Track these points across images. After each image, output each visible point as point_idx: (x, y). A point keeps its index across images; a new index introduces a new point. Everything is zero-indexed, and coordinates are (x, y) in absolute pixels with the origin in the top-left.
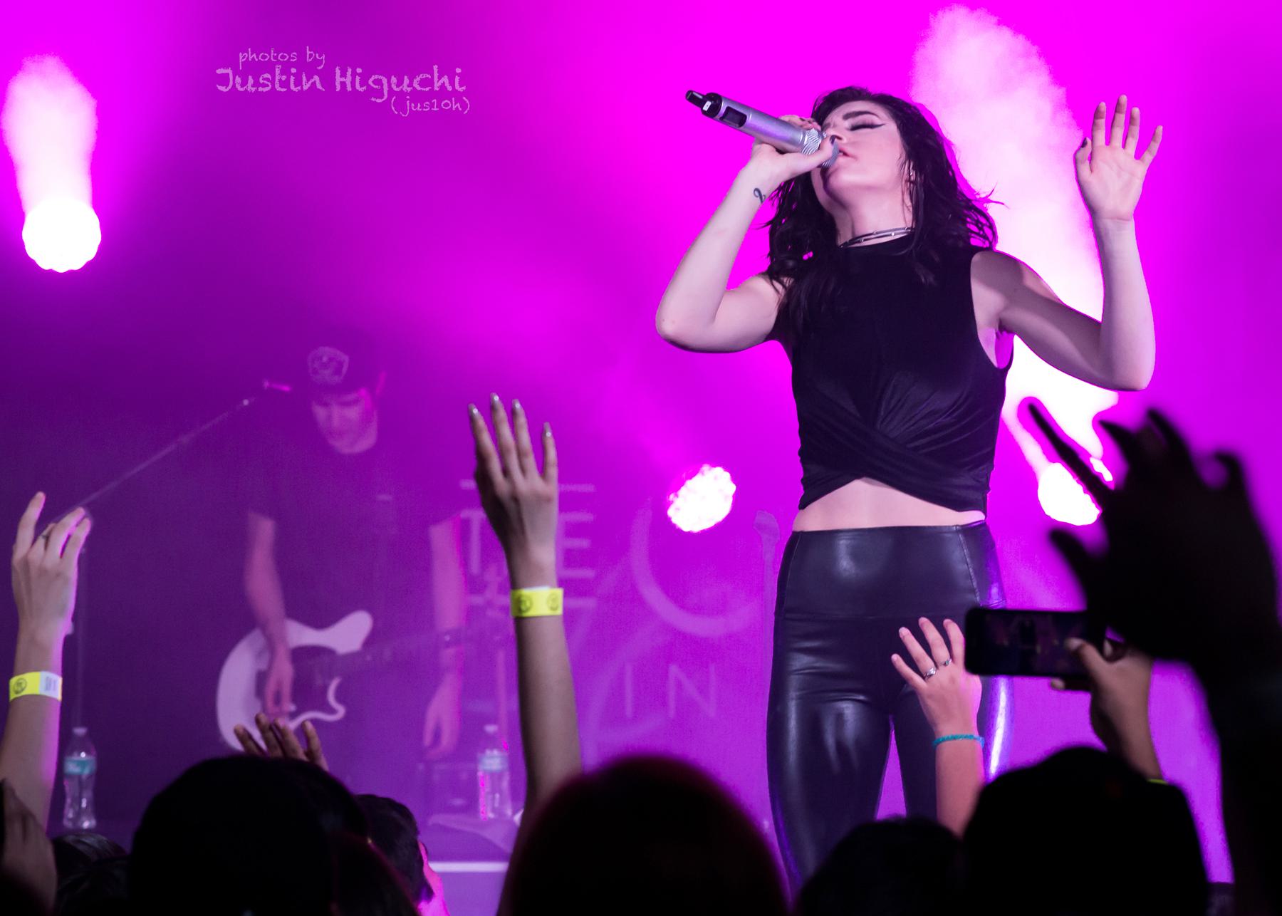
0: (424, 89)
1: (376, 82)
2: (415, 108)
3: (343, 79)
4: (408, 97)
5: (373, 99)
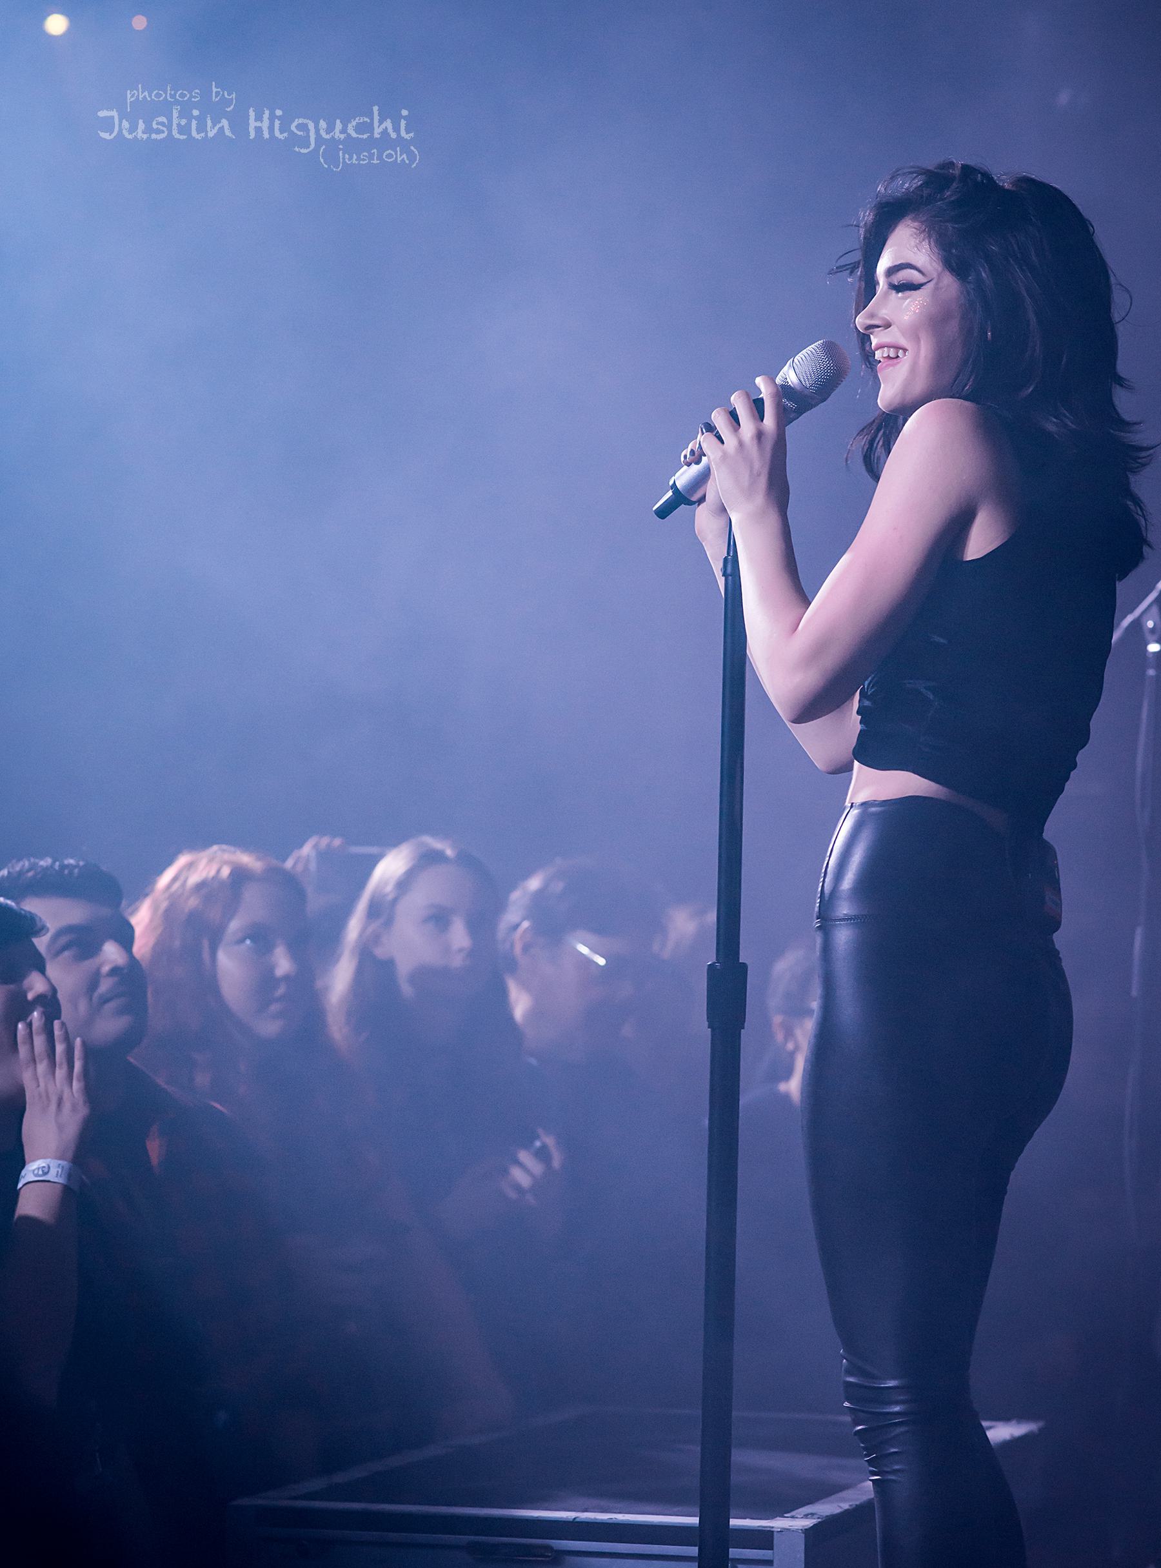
0: (360, 136)
1: (300, 127)
2: (349, 160)
3: (258, 124)
4: (341, 147)
5: (297, 149)
